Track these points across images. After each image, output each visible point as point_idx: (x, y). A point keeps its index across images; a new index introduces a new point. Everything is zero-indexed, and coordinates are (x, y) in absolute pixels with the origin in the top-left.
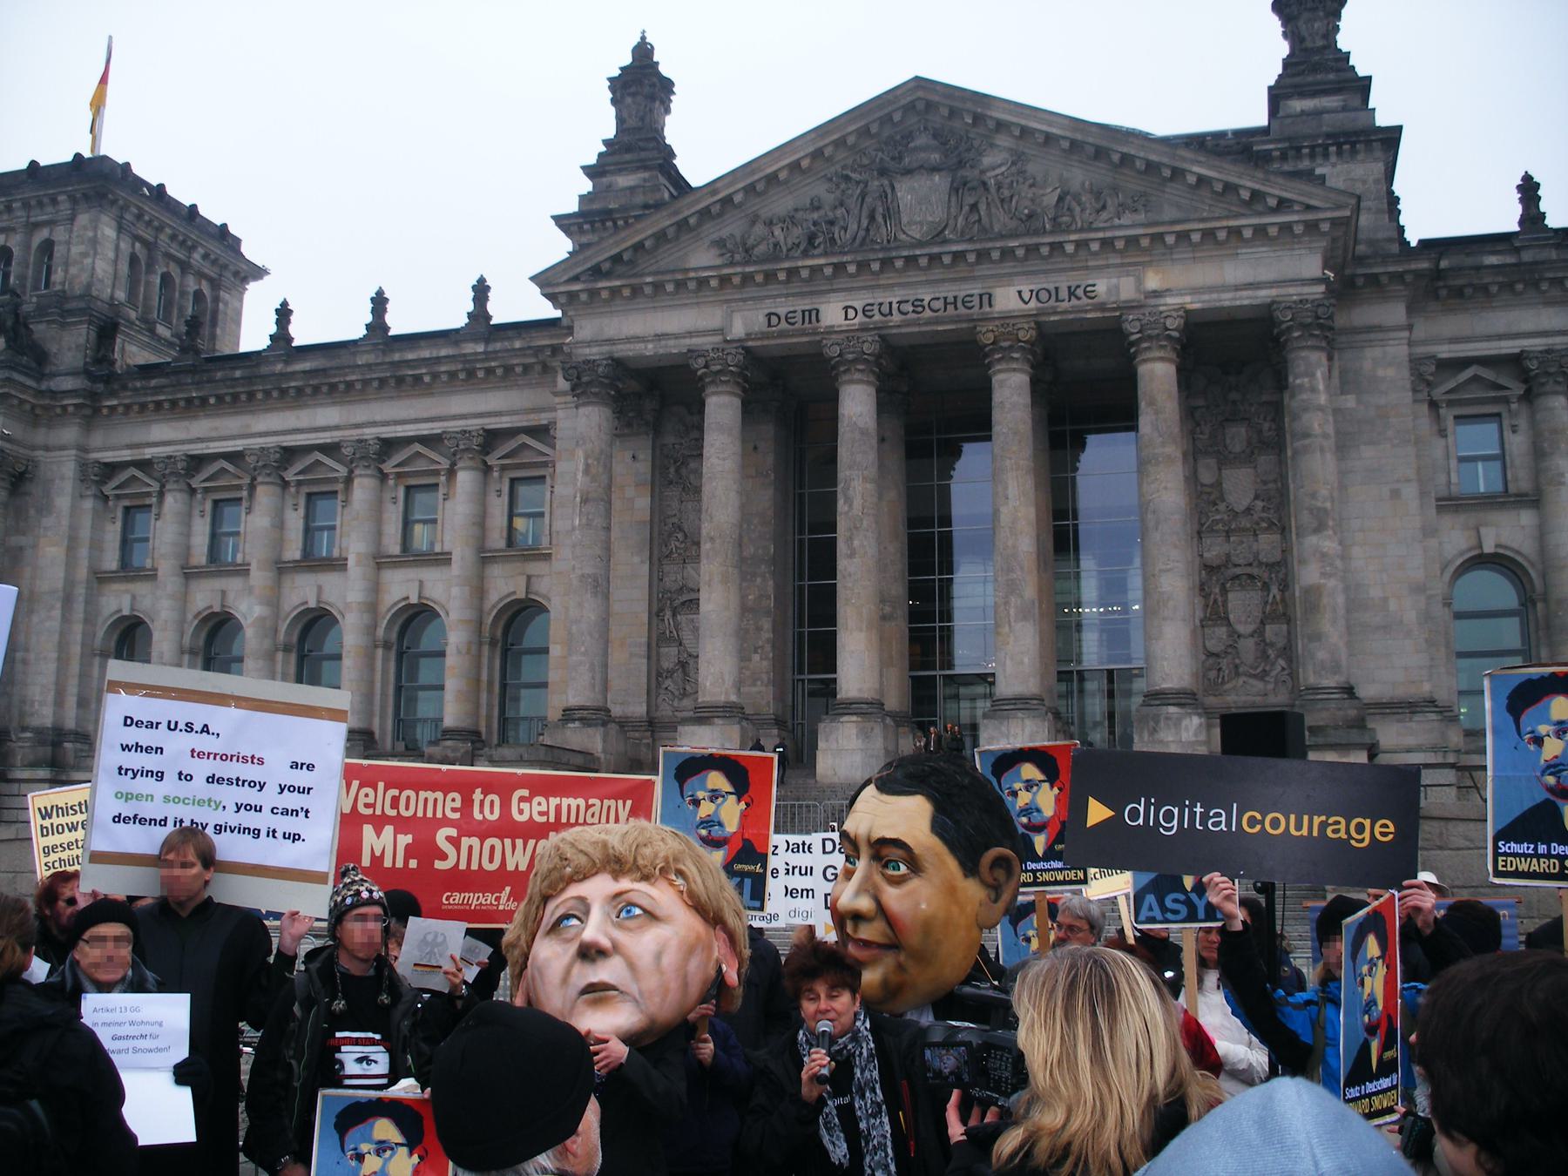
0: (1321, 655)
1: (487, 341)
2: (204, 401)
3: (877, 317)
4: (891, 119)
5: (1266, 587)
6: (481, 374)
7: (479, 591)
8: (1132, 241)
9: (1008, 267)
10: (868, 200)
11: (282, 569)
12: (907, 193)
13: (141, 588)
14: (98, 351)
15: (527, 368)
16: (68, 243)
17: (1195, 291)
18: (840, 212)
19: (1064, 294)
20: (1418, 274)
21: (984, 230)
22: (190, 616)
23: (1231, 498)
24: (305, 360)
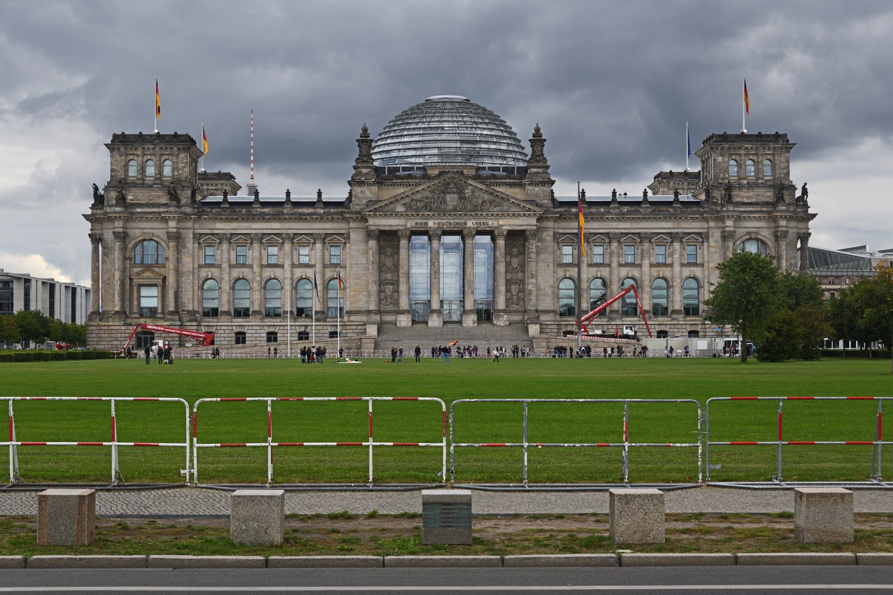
0: (531, 303)
1: (324, 209)
2: (238, 218)
4: (445, 180)
5: (520, 285)
7: (324, 276)
9: (471, 217)
10: (440, 199)
11: (262, 266)
12: (449, 197)
13: (214, 270)
14: (192, 198)
15: (338, 218)
16: (177, 163)
17: (510, 225)
18: (433, 200)
19: (482, 224)
20: (556, 217)
21: (466, 209)
22: (231, 279)
23: (513, 265)
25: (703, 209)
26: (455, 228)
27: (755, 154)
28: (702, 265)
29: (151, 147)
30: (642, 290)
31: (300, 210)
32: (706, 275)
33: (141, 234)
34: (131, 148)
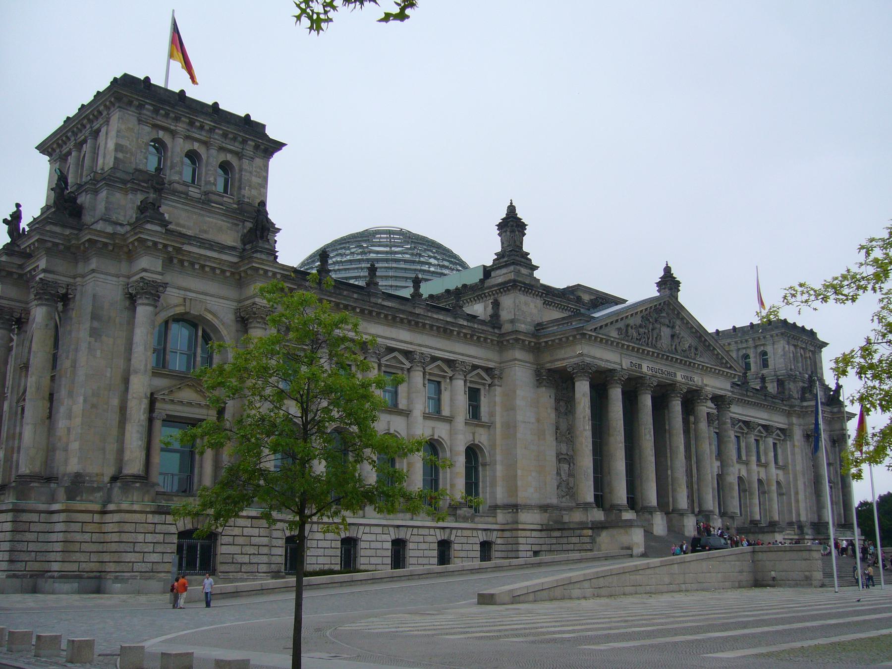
1: (468, 321)
2: (354, 309)
3: (654, 373)
6: (475, 338)
8: (707, 367)
9: (682, 366)
10: (657, 331)
15: (492, 340)
17: (712, 387)
24: (390, 301)
25: (782, 401)
26: (666, 379)
27: (803, 348)
28: (784, 468)
29: (209, 123)
30: (751, 494)
31: (435, 316)
32: (791, 479)
33: (181, 301)
34: (167, 116)
